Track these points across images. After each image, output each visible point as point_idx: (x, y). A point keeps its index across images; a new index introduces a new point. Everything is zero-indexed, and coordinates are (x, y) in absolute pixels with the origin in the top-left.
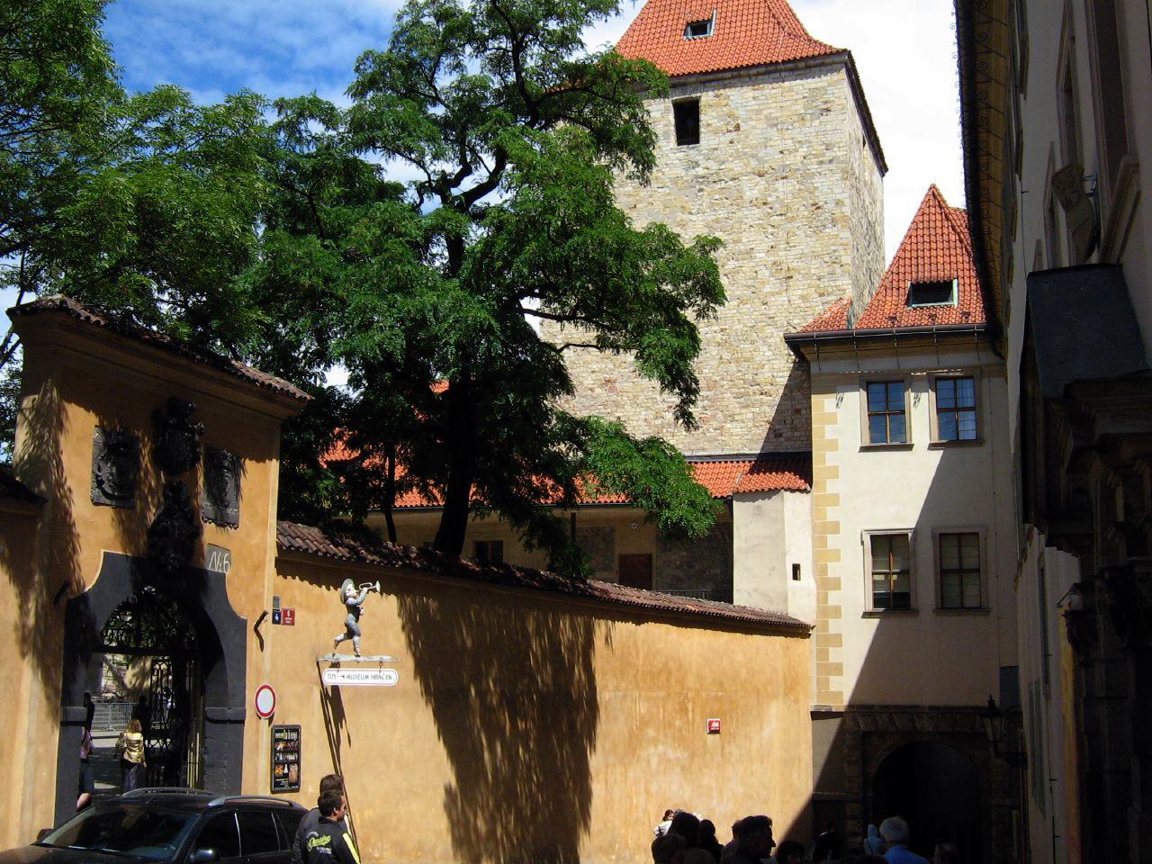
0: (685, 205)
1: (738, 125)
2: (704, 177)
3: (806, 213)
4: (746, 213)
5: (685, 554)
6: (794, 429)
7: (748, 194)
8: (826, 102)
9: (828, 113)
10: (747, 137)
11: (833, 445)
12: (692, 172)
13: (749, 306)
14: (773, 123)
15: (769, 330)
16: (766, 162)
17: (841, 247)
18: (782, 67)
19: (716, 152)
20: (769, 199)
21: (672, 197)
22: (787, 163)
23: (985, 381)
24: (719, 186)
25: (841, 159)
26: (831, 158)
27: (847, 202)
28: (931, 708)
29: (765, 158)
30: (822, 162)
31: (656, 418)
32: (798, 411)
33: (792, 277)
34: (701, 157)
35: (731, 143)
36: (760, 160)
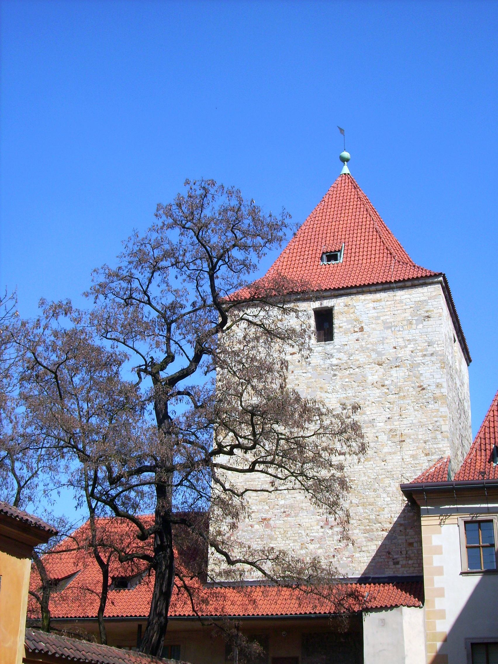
0: (323, 386)
1: (362, 327)
2: (337, 366)
3: (414, 393)
4: (369, 392)
5: (324, 657)
6: (408, 558)
7: (370, 378)
8: (427, 311)
9: (429, 319)
10: (369, 336)
11: (440, 571)
12: (328, 361)
13: (372, 462)
14: (388, 326)
15: (387, 481)
16: (384, 354)
17: (441, 419)
18: (394, 285)
19: (346, 347)
20: (386, 383)
21: (313, 380)
22: (399, 355)
24: (348, 372)
25: (440, 353)
26: (432, 352)
27: (445, 385)
29: (383, 352)
31: (302, 548)
32: (411, 544)
33: (404, 441)
34: (335, 351)
35: (357, 340)
36: (379, 354)
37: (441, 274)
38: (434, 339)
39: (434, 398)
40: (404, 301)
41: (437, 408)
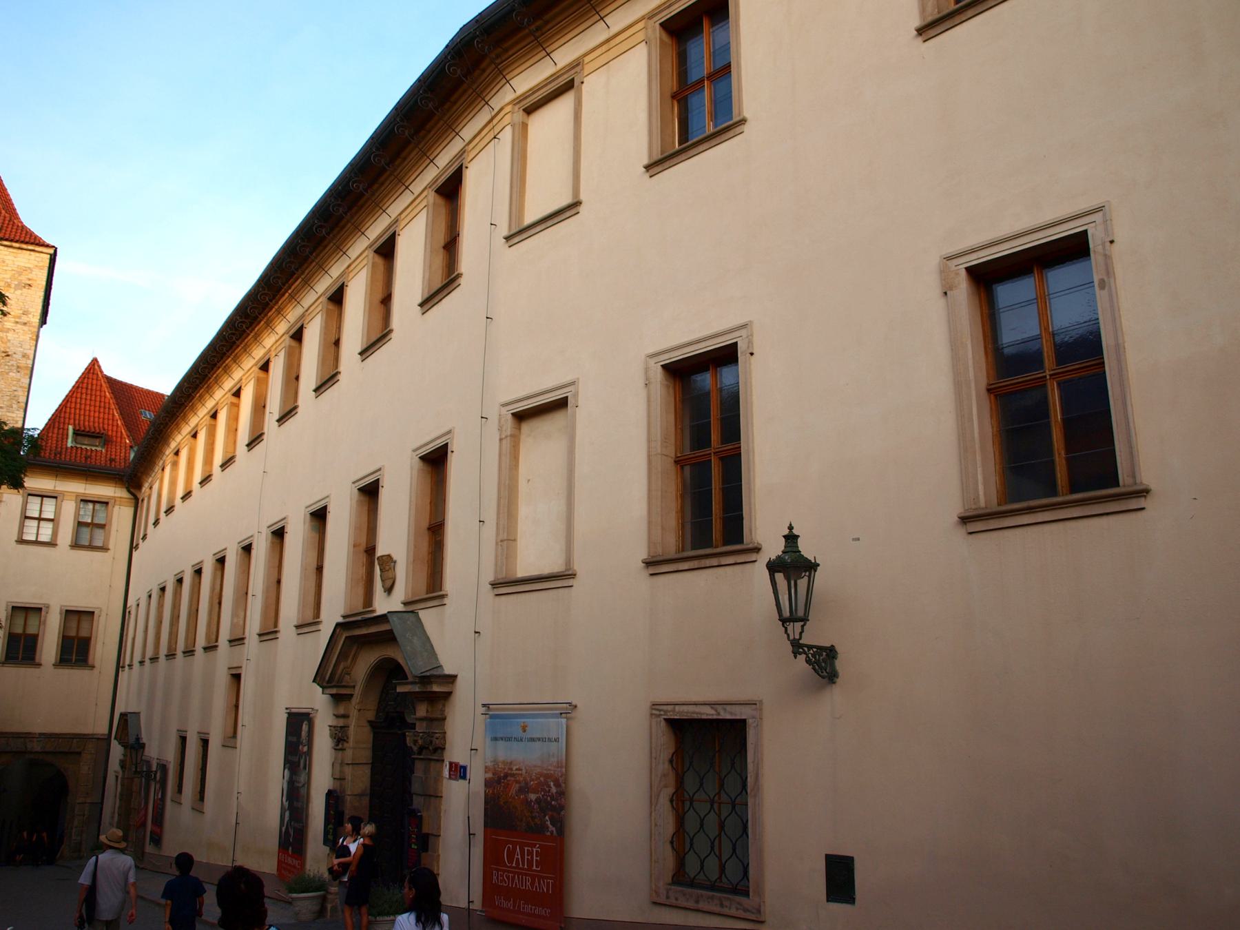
8: (29, 279)
17: (19, 389)
23: (117, 508)
26: (26, 321)
28: (40, 734)
30: (17, 322)
37: (53, 247)
38: (31, 310)
39: (18, 367)
40: (7, 262)
41: (19, 378)
